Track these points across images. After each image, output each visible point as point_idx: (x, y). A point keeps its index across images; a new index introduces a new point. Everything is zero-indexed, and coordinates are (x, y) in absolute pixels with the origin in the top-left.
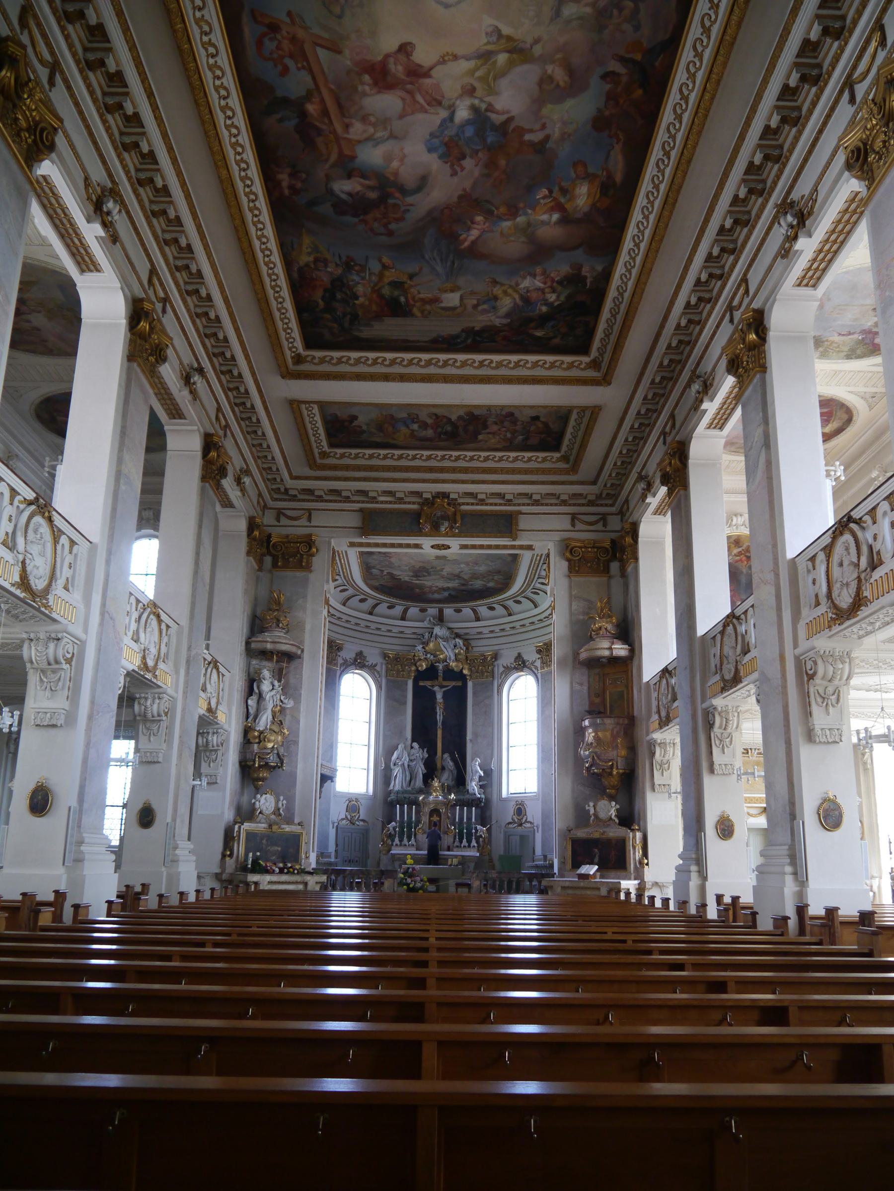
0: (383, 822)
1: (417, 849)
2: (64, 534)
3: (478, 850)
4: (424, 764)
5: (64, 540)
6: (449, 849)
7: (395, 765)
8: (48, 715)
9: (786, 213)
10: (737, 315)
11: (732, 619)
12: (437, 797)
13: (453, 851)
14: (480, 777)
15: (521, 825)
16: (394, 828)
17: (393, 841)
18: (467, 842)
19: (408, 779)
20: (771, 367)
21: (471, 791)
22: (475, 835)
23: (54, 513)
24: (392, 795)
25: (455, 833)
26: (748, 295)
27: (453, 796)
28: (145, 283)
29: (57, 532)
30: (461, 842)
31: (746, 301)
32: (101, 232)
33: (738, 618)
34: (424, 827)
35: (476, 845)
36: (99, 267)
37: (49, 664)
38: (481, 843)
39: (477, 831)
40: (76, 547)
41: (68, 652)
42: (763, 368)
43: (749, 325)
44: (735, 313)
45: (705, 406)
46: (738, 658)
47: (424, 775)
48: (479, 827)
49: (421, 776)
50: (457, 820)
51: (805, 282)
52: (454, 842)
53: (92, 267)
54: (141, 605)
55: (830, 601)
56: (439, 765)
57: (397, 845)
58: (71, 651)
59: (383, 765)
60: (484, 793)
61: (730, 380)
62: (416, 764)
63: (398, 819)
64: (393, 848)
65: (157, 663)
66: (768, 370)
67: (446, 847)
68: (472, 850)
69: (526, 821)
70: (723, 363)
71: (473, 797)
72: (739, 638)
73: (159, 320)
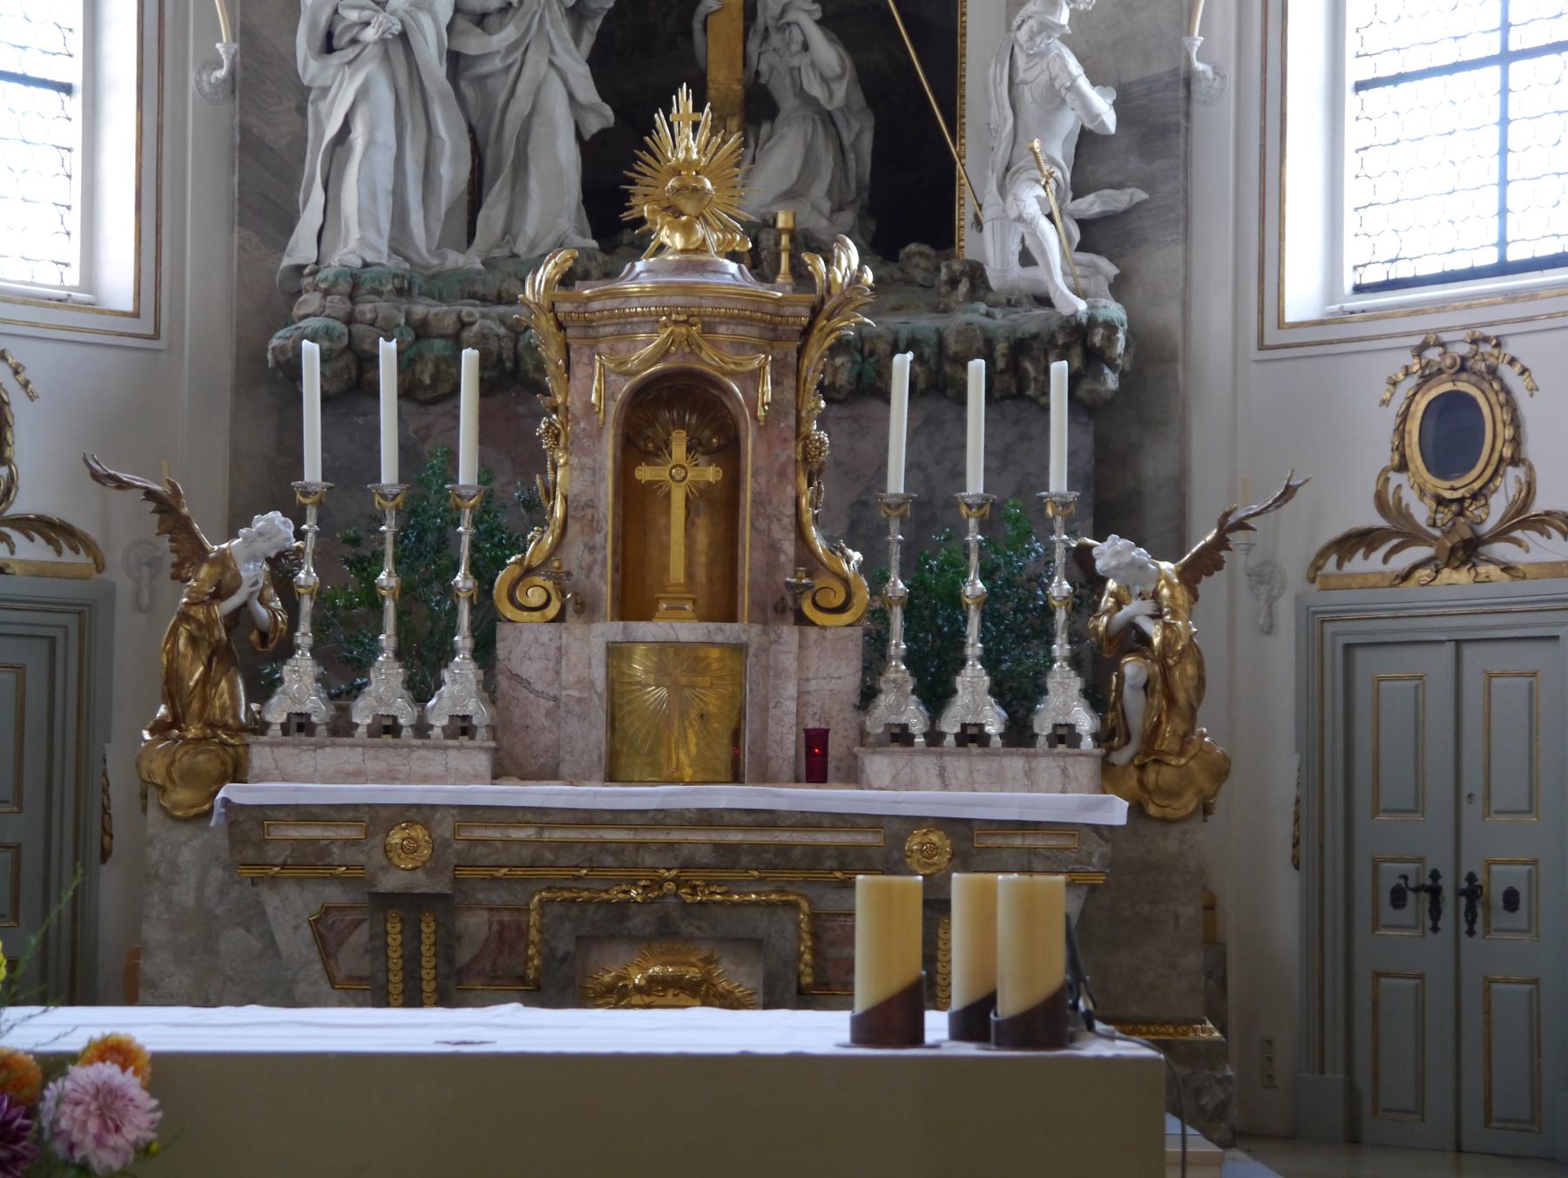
0: (166, 507)
1: (498, 773)
3: (1108, 777)
4: (597, 62)
6: (815, 769)
7: (329, 45)
12: (693, 260)
13: (853, 776)
14: (1088, 141)
15: (1467, 551)
16: (281, 568)
17: (263, 689)
18: (997, 691)
19: (452, 172)
21: (1002, 268)
22: (1074, 637)
24: (310, 301)
25: (879, 616)
27: (850, 256)
30: (936, 694)
34: (575, 556)
35: (1085, 721)
38: (1133, 701)
39: (1088, 580)
47: (591, 148)
48: (1110, 552)
49: (568, 154)
50: (896, 483)
52: (868, 695)
56: (723, 75)
57: (300, 725)
59: (224, 48)
60: (1118, 288)
62: (520, 46)
63: (313, 470)
64: (260, 756)
67: (786, 744)
68: (1048, 765)
69: (1522, 518)
71: (1031, 321)
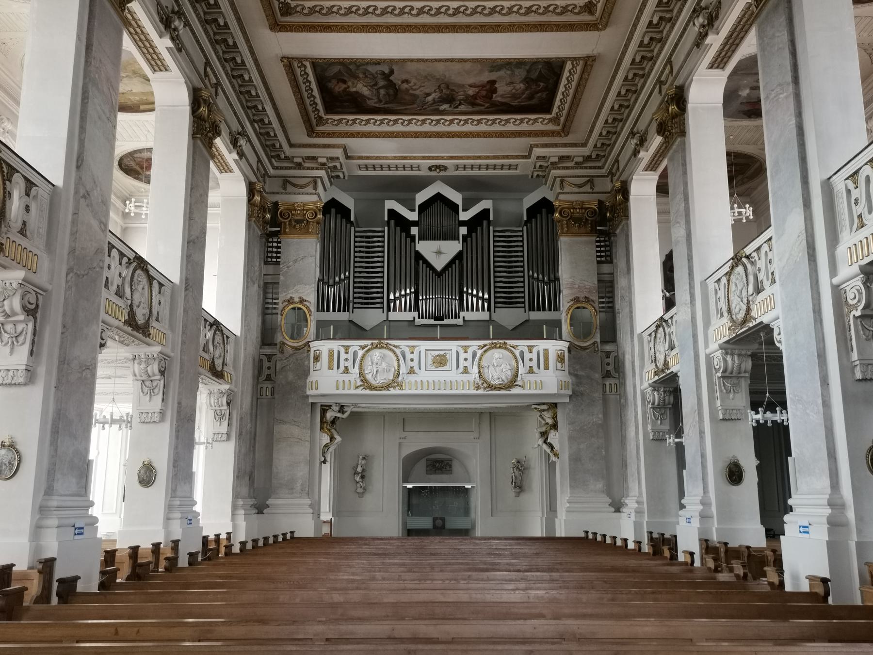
2: (155, 279)
5: (155, 285)
8: (150, 414)
9: (698, 16)
10: (664, 88)
11: (662, 322)
20: (689, 132)
23: (148, 266)
26: (672, 75)
28: (202, 73)
29: (151, 279)
31: (671, 79)
32: (170, 44)
33: (666, 321)
36: (167, 68)
37: (149, 376)
40: (163, 287)
41: (162, 367)
42: (683, 133)
43: (672, 99)
44: (663, 87)
45: (642, 154)
46: (667, 353)
51: (716, 65)
53: (162, 68)
54: (208, 323)
55: (729, 316)
58: (164, 366)
61: (658, 140)
65: (223, 368)
66: (687, 135)
70: (654, 126)
72: (667, 337)
73: (215, 103)
